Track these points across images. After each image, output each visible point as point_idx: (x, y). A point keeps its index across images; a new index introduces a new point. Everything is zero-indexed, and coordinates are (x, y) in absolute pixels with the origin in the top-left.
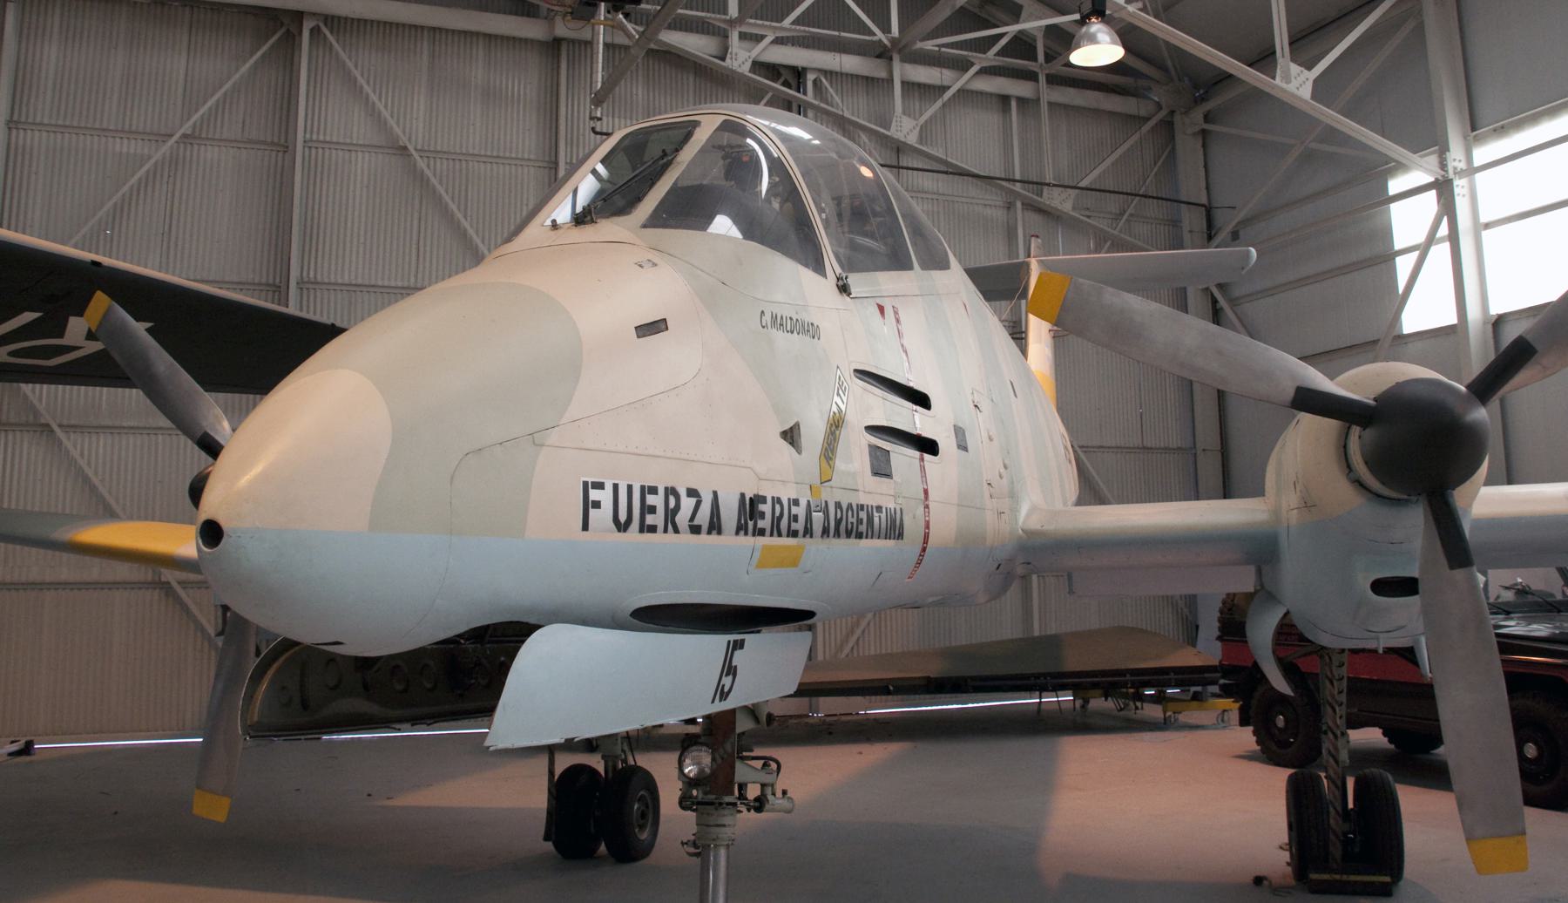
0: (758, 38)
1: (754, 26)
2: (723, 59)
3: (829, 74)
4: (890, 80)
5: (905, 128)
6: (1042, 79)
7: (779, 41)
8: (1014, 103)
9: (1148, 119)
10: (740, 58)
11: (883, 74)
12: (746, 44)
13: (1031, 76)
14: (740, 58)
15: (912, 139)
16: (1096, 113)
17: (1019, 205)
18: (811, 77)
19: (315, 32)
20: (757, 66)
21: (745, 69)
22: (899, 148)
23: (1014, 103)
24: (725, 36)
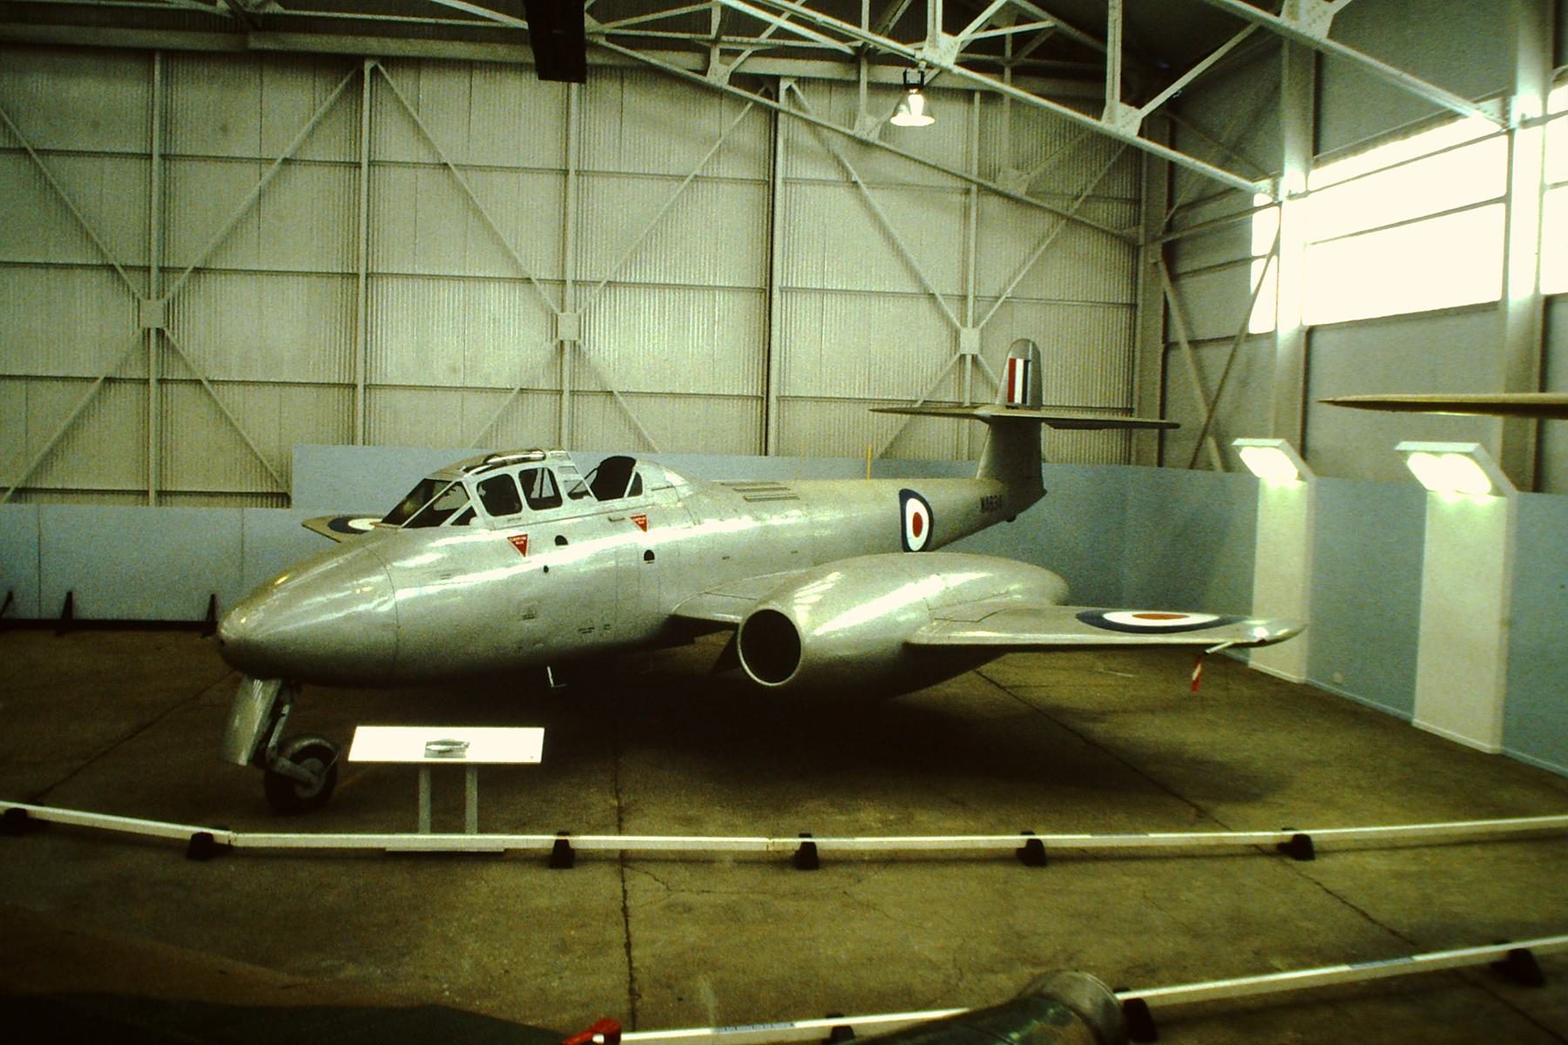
0: (738, 53)
2: (704, 73)
3: (801, 81)
4: (858, 81)
7: (755, 54)
8: (977, 96)
11: (853, 78)
12: (727, 59)
17: (974, 188)
18: (784, 85)
19: (375, 71)
20: (737, 78)
21: (723, 83)
22: (865, 144)
23: (977, 96)
24: (706, 53)
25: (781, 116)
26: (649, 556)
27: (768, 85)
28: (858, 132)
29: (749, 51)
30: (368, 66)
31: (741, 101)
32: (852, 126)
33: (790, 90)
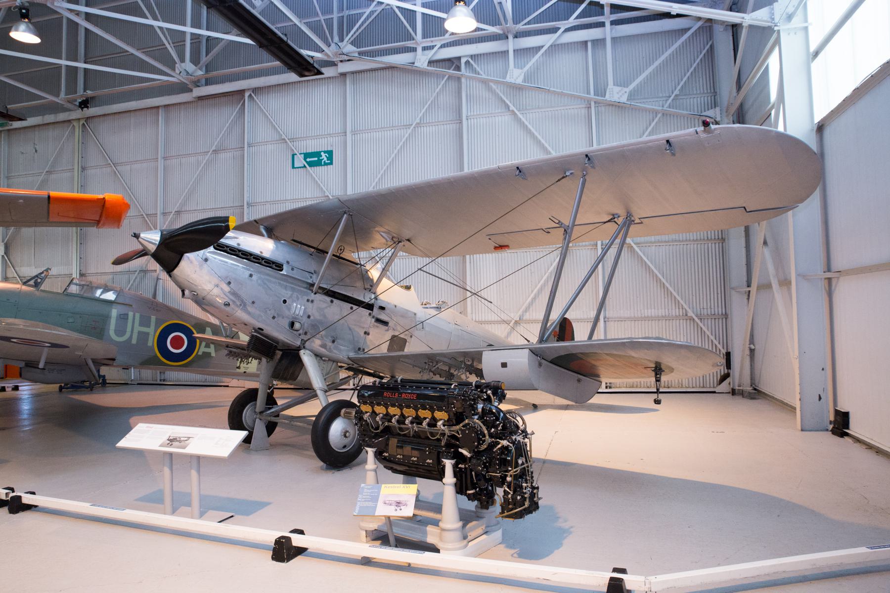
0: (433, 47)
1: (427, 42)
5: (516, 75)
6: (608, 24)
9: (689, 29)
10: (422, 60)
11: (504, 49)
12: (426, 52)
13: (602, 25)
14: (422, 60)
15: (519, 81)
16: (656, 34)
17: (593, 104)
18: (463, 61)
23: (589, 44)
24: (414, 50)
25: (463, 80)
26: (504, 365)
27: (453, 63)
28: (508, 79)
29: (439, 46)
30: (247, 94)
31: (439, 76)
32: (505, 77)
33: (467, 63)
